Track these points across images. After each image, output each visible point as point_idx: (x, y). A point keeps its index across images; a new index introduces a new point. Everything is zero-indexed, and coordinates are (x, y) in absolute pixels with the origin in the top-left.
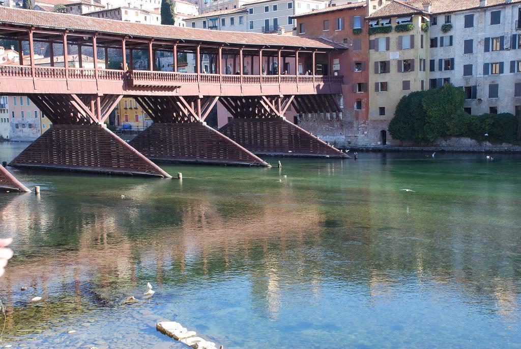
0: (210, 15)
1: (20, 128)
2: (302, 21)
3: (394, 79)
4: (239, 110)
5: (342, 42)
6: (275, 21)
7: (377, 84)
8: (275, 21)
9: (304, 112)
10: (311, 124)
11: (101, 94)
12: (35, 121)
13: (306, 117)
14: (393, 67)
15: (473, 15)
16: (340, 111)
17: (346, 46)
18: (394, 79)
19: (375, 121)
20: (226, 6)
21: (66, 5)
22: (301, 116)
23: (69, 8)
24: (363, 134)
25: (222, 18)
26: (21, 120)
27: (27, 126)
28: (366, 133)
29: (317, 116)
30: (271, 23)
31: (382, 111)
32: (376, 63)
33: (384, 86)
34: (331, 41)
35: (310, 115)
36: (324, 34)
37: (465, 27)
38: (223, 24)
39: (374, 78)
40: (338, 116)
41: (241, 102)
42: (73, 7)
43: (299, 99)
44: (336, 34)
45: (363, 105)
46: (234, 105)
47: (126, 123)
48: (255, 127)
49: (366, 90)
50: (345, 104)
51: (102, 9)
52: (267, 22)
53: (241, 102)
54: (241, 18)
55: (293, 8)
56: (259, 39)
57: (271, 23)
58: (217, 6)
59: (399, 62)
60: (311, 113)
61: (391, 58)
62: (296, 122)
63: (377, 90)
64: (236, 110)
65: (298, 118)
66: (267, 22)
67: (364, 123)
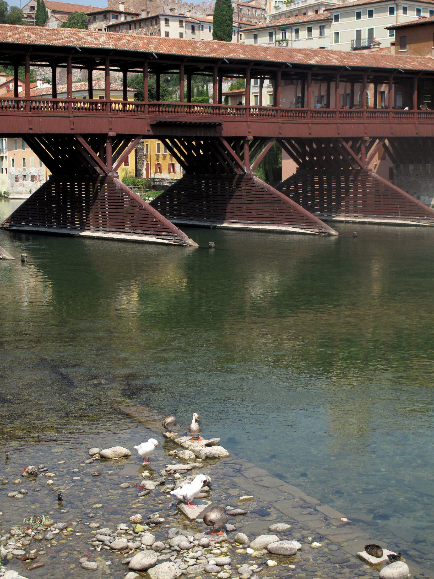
0: (278, 24)
1: (20, 181)
4: (307, 159)
6: (371, 31)
8: (371, 31)
11: (112, 134)
12: (38, 172)
20: (304, 11)
21: (88, 15)
22: (397, 167)
23: (92, 18)
26: (21, 170)
27: (29, 178)
29: (421, 168)
30: (365, 35)
35: (411, 167)
41: (311, 147)
42: (97, 17)
43: (396, 144)
46: (300, 150)
47: (158, 176)
48: (329, 183)
51: (135, 18)
52: (359, 33)
53: (311, 147)
56: (337, 59)
57: (365, 35)
58: (290, 12)
62: (391, 177)
64: (304, 159)
65: (395, 171)
66: (359, 33)
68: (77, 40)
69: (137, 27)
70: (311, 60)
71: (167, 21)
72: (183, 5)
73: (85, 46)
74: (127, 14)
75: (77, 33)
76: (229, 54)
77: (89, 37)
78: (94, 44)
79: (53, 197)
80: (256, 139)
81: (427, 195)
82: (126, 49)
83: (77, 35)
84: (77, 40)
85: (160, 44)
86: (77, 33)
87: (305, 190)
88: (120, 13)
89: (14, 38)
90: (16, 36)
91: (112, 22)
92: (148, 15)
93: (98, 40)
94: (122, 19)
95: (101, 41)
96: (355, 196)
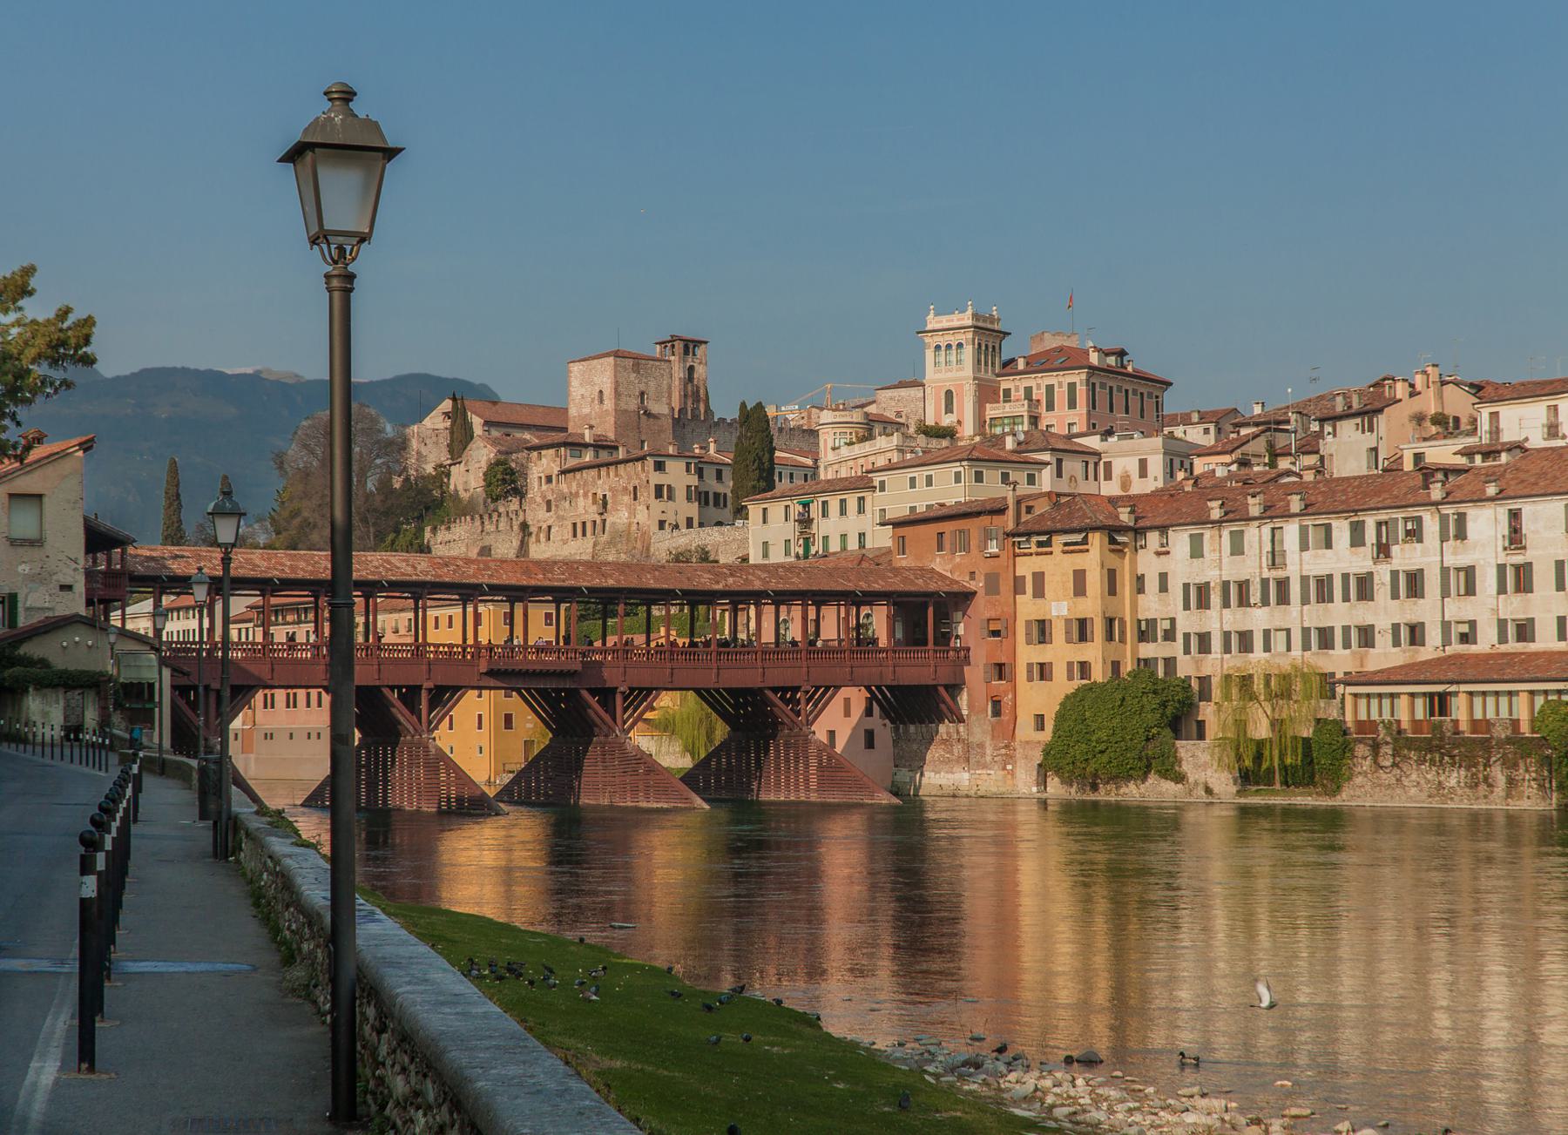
2: (902, 531)
3: (1060, 652)
5: (967, 578)
7: (1030, 666)
9: (904, 723)
10: (915, 747)
13: (906, 731)
14: (1058, 632)
15: (1202, 534)
16: (961, 720)
17: (972, 586)
18: (1060, 652)
19: (1027, 742)
24: (1004, 769)
25: (824, 499)
28: (1009, 767)
31: (1040, 721)
32: (1028, 623)
33: (1044, 671)
34: (949, 575)
35: (912, 728)
36: (938, 560)
37: (1191, 557)
38: (825, 514)
39: (1027, 654)
40: (958, 732)
42: (543, 452)
44: (958, 560)
45: (1006, 710)
49: (1013, 680)
50: (970, 706)
54: (861, 499)
55: (963, 484)
59: (1068, 621)
60: (913, 722)
61: (1054, 613)
63: (1030, 679)
67: (1007, 747)
68: (387, 570)
69: (612, 474)
70: (718, 583)
71: (659, 467)
72: (717, 424)
73: (394, 578)
74: (599, 445)
75: (391, 558)
76: (593, 579)
77: (404, 564)
78: (407, 575)
79: (364, 766)
80: (632, 690)
81: (933, 771)
82: (447, 580)
83: (389, 562)
84: (387, 570)
85: (502, 568)
86: (391, 558)
87: (739, 760)
88: (591, 445)
89: (306, 572)
90: (310, 568)
91: (572, 462)
92: (642, 448)
93: (414, 568)
94: (588, 457)
95: (419, 567)
96: (796, 768)
